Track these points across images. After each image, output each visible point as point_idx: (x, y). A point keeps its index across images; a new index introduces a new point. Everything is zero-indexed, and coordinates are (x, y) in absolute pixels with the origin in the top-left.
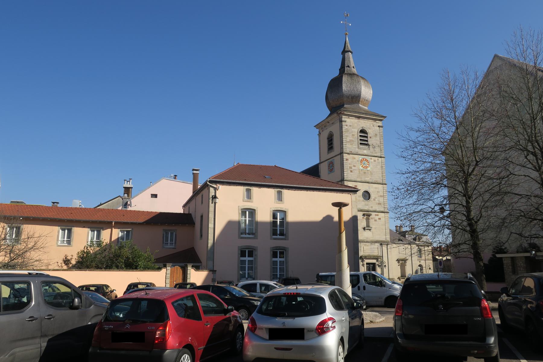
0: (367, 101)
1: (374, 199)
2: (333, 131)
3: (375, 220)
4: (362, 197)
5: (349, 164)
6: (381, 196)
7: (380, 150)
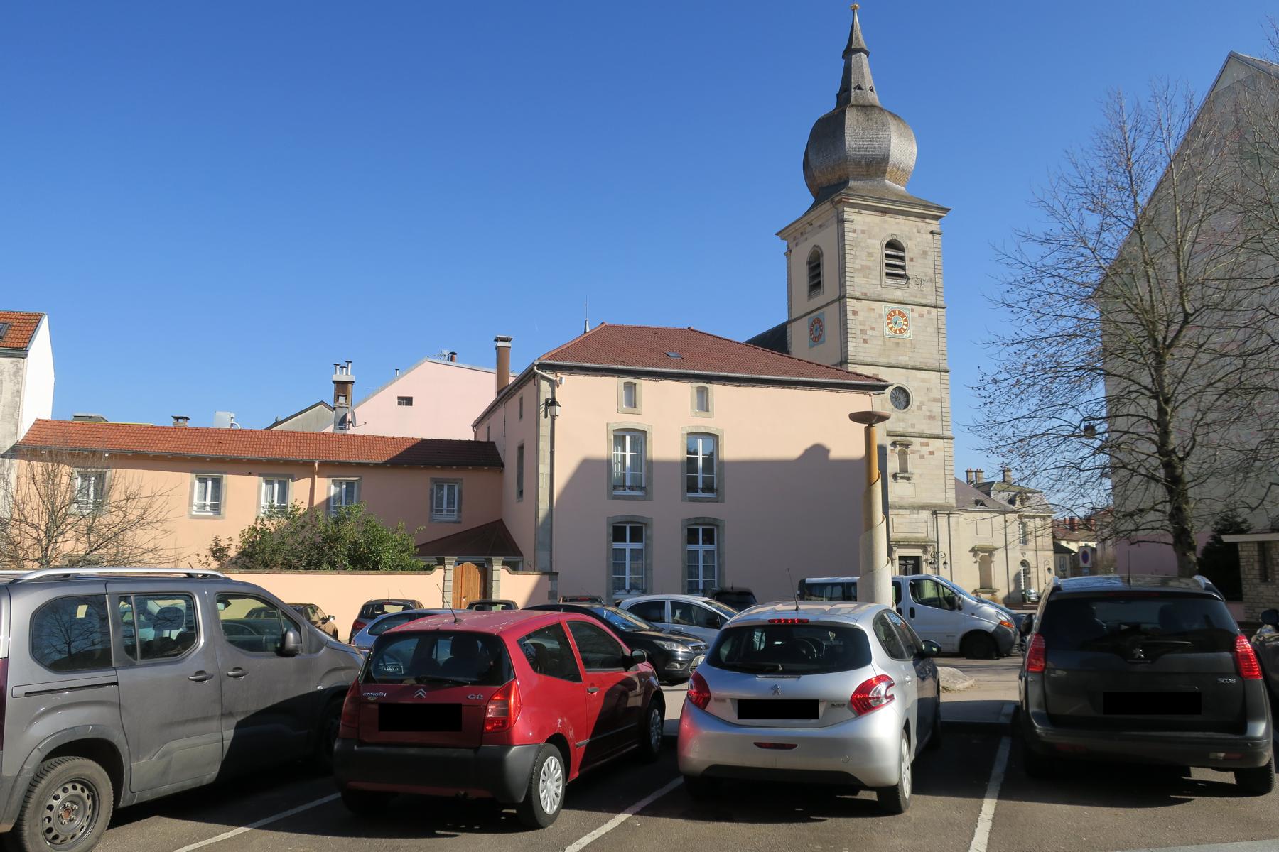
0: (903, 170)
1: (918, 406)
2: (821, 246)
5: (860, 325)
6: (935, 400)
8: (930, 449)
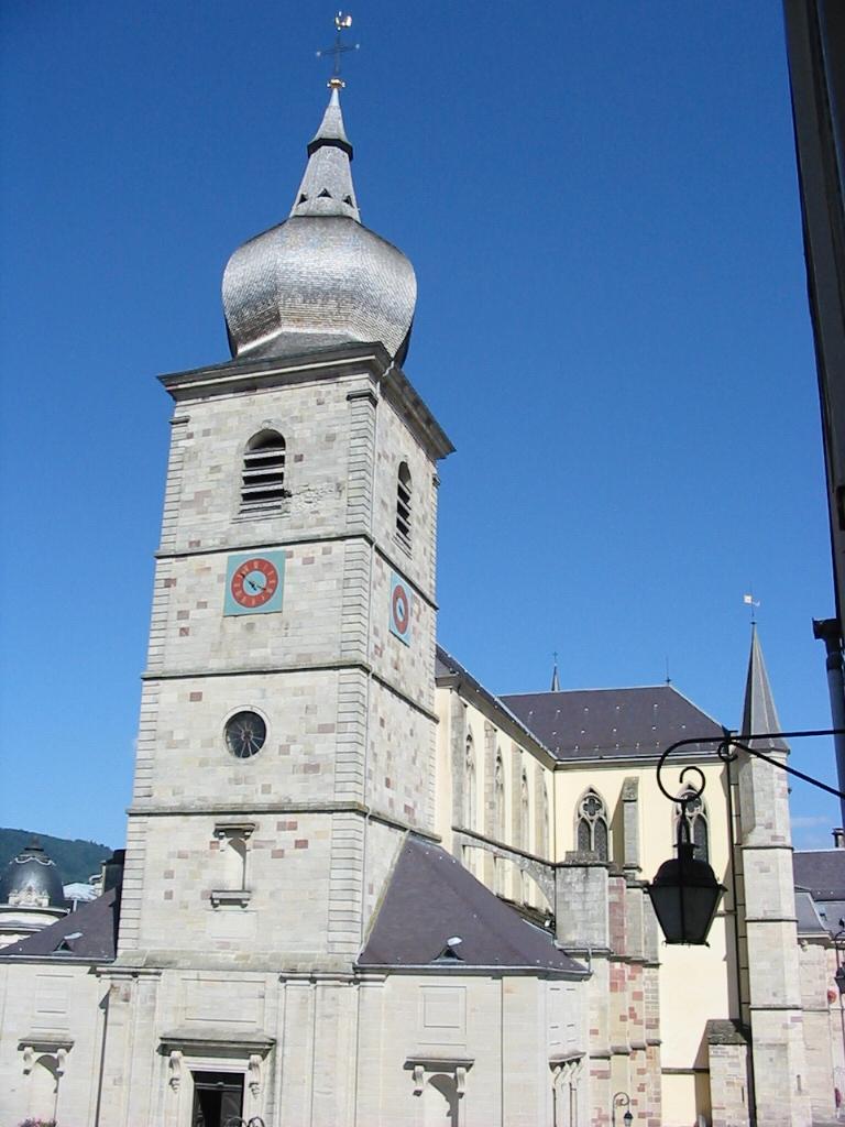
1: (281, 747)
3: (273, 852)
5: (179, 602)
6: (324, 729)
8: (299, 835)
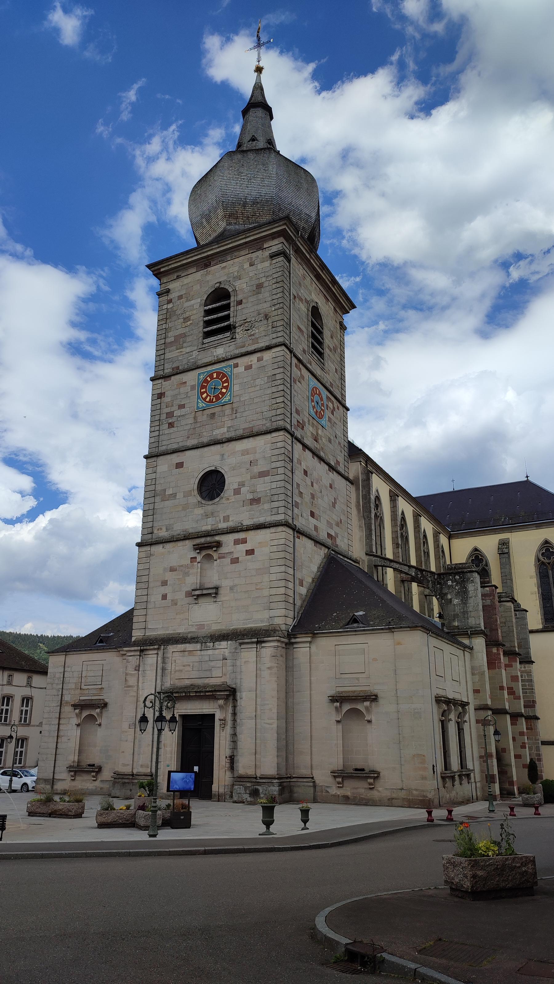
4: (196, 492)
6: (263, 474)
7: (270, 327)
8: (248, 546)
